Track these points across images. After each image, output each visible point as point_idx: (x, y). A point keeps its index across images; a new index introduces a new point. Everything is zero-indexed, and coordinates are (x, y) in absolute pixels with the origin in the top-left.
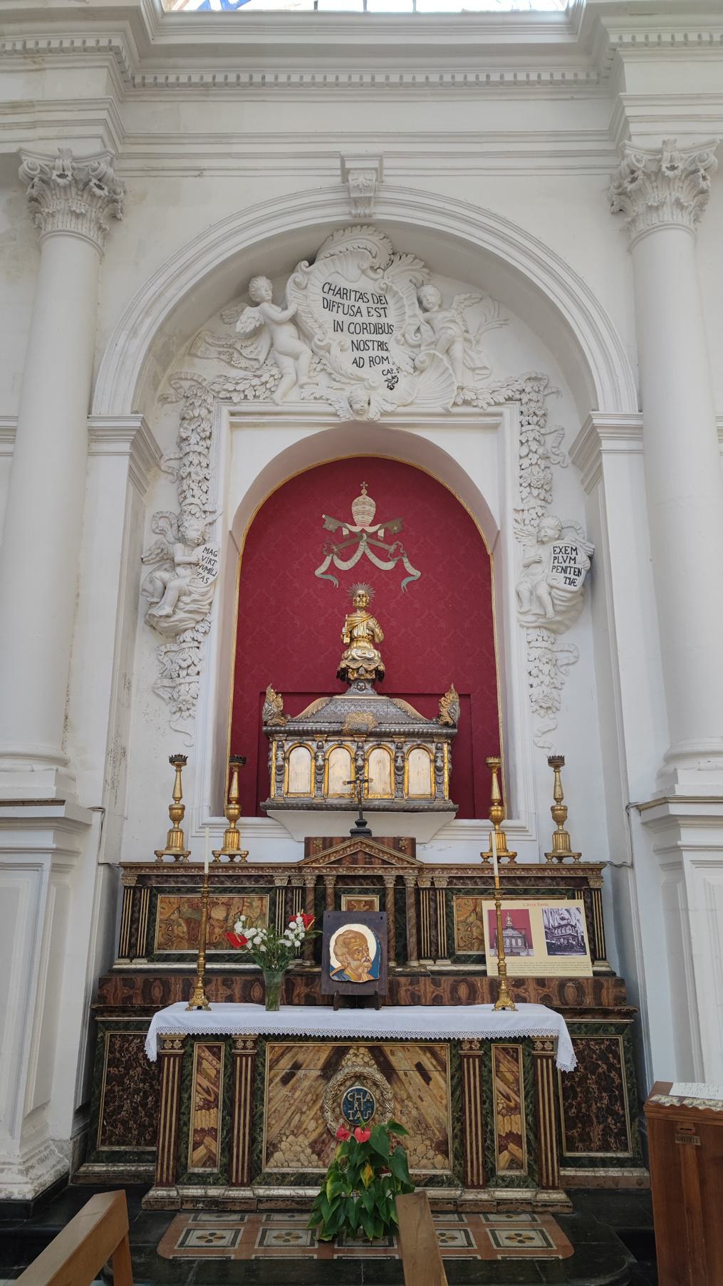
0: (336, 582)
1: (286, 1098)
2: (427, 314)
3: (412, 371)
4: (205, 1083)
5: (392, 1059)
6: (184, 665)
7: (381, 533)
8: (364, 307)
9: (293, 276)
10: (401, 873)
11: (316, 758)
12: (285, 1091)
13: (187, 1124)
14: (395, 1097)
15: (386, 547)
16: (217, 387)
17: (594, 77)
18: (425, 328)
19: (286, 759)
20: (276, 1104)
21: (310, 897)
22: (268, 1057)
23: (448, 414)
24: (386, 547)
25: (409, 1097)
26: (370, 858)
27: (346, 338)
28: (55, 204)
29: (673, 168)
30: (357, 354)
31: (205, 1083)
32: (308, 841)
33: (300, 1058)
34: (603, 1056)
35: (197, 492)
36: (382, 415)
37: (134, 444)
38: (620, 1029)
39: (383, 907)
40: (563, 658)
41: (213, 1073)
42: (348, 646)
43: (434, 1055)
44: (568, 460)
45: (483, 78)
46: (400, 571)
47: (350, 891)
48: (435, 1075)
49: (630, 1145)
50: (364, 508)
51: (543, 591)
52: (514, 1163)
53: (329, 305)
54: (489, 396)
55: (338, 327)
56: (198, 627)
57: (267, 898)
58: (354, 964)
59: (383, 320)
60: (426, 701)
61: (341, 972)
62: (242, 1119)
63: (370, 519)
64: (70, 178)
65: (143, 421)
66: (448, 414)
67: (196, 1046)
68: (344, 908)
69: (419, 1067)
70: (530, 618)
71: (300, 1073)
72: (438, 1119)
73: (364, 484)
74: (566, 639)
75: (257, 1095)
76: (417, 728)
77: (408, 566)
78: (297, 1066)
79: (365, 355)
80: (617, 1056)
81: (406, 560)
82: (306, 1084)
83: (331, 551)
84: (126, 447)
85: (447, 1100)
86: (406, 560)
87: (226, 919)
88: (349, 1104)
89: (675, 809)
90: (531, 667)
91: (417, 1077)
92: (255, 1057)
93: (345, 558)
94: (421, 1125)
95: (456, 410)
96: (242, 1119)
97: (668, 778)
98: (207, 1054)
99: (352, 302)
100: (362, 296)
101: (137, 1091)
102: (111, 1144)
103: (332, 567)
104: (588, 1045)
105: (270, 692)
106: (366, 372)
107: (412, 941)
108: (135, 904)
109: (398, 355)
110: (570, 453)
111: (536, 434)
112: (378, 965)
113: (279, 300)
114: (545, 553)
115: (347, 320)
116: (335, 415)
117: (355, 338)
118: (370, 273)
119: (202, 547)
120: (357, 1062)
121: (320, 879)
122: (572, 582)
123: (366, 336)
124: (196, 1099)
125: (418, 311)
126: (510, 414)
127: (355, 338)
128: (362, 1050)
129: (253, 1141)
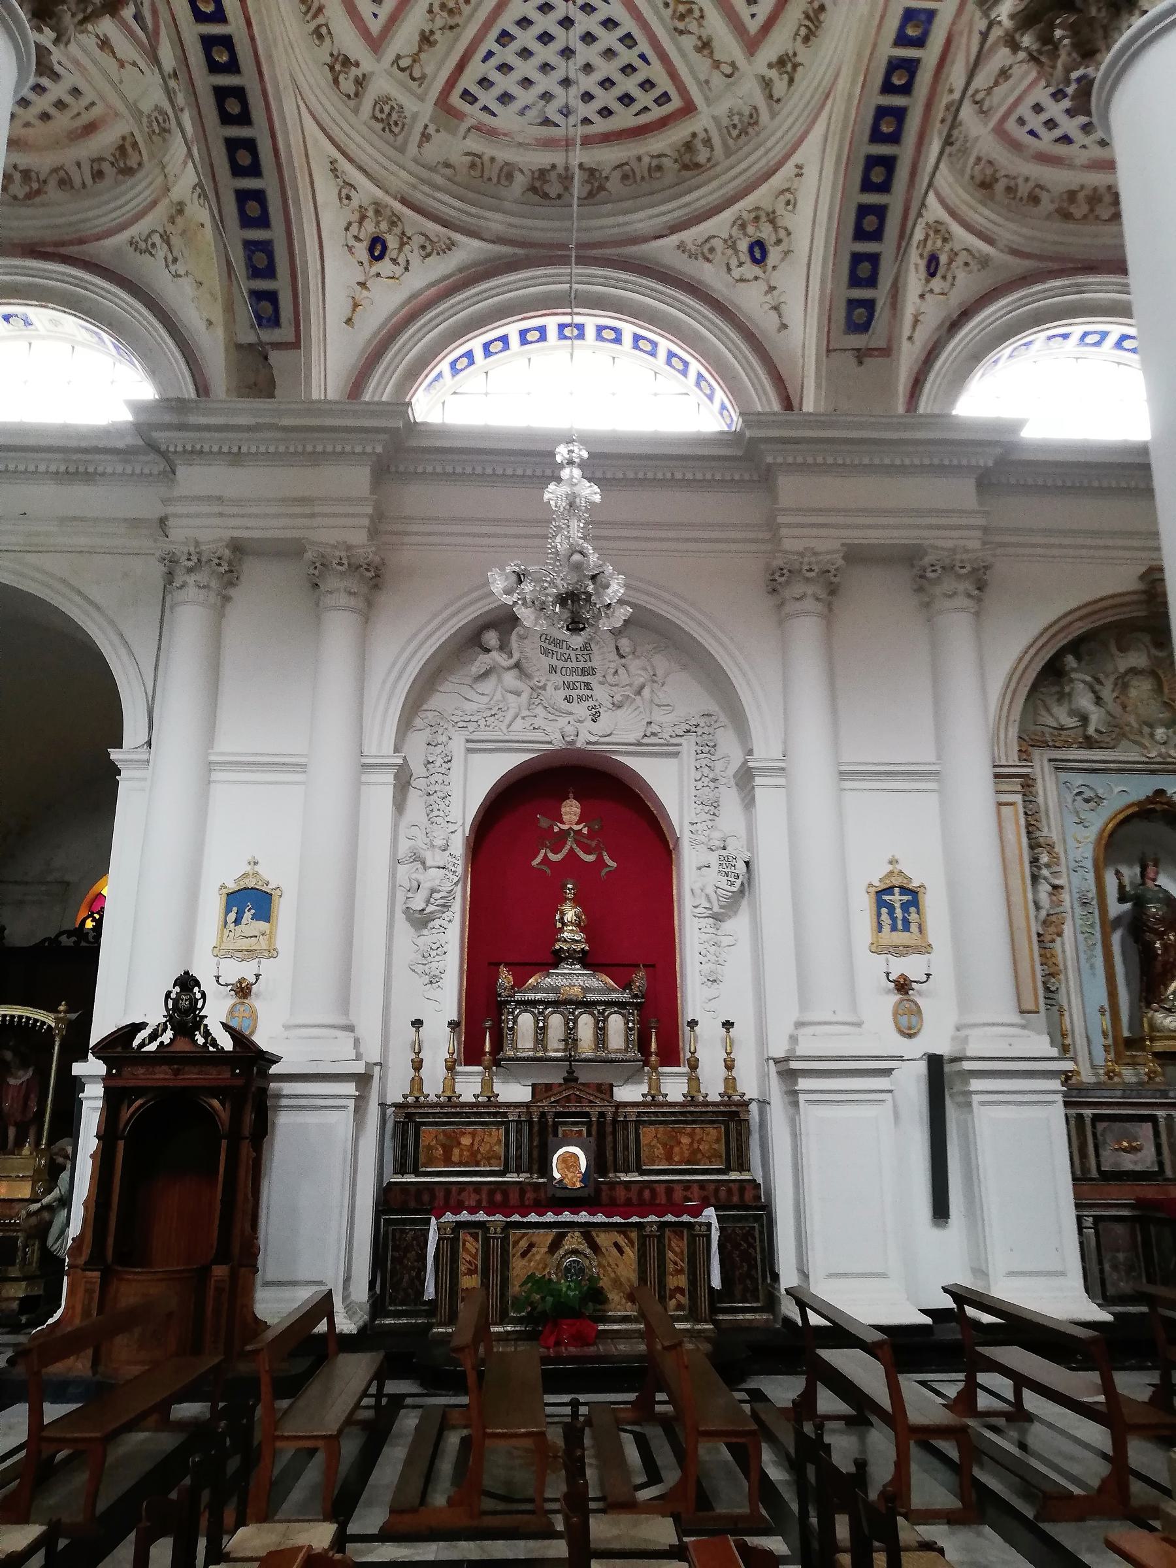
0: (548, 871)
1: (524, 1267)
2: (623, 661)
3: (611, 706)
4: (468, 1258)
5: (597, 1239)
6: (434, 947)
7: (585, 831)
9: (517, 629)
10: (603, 1109)
11: (537, 1021)
12: (524, 1262)
13: (457, 1284)
14: (600, 1265)
15: (589, 842)
16: (455, 718)
17: (756, 478)
18: (622, 671)
19: (515, 1022)
20: (515, 1273)
21: (536, 1128)
22: (512, 1239)
23: (639, 744)
24: (589, 842)
25: (609, 1265)
26: (579, 1099)
27: (558, 679)
28: (331, 582)
29: (811, 570)
30: (568, 692)
31: (468, 1258)
32: (534, 1086)
33: (534, 1239)
35: (442, 806)
36: (588, 743)
37: (396, 776)
39: (589, 1134)
40: (726, 941)
41: (473, 1251)
42: (561, 930)
43: (627, 1237)
44: (733, 782)
45: (669, 476)
46: (600, 862)
47: (565, 1123)
48: (627, 1250)
49: (761, 1297)
50: (571, 811)
51: (710, 890)
52: (679, 1307)
53: (546, 652)
54: (671, 729)
55: (552, 669)
56: (444, 916)
57: (502, 1129)
58: (570, 1175)
59: (589, 664)
60: (620, 972)
61: (561, 1181)
62: (495, 1280)
63: (576, 819)
64: (346, 566)
65: (405, 759)
66: (639, 744)
67: (461, 1232)
68: (560, 1135)
69: (616, 1245)
70: (700, 910)
71: (534, 1250)
72: (629, 1280)
74: (728, 926)
75: (505, 1263)
76: (614, 997)
77: (606, 857)
78: (531, 1246)
79: (574, 693)
80: (754, 1238)
82: (538, 1257)
83: (544, 846)
84: (390, 778)
85: (635, 1266)
87: (472, 1144)
88: (567, 1269)
89: (794, 1065)
90: (701, 948)
91: (615, 1251)
92: (502, 1238)
94: (617, 1283)
95: (646, 740)
96: (495, 1280)
97: (794, 1039)
98: (469, 1238)
99: (564, 650)
101: (413, 1268)
102: (396, 1305)
103: (546, 860)
104: (734, 1230)
105: (503, 970)
107: (610, 1158)
108: (405, 1133)
109: (601, 694)
110: (734, 776)
111: (707, 762)
112: (585, 1177)
113: (504, 647)
114: (713, 858)
115: (560, 664)
116: (550, 743)
117: (567, 679)
119: (447, 853)
120: (573, 1241)
121: (543, 1115)
122: (732, 884)
123: (575, 678)
124: (463, 1268)
125: (617, 657)
126: (688, 745)
127: (567, 679)
128: (577, 1234)
129: (503, 1295)
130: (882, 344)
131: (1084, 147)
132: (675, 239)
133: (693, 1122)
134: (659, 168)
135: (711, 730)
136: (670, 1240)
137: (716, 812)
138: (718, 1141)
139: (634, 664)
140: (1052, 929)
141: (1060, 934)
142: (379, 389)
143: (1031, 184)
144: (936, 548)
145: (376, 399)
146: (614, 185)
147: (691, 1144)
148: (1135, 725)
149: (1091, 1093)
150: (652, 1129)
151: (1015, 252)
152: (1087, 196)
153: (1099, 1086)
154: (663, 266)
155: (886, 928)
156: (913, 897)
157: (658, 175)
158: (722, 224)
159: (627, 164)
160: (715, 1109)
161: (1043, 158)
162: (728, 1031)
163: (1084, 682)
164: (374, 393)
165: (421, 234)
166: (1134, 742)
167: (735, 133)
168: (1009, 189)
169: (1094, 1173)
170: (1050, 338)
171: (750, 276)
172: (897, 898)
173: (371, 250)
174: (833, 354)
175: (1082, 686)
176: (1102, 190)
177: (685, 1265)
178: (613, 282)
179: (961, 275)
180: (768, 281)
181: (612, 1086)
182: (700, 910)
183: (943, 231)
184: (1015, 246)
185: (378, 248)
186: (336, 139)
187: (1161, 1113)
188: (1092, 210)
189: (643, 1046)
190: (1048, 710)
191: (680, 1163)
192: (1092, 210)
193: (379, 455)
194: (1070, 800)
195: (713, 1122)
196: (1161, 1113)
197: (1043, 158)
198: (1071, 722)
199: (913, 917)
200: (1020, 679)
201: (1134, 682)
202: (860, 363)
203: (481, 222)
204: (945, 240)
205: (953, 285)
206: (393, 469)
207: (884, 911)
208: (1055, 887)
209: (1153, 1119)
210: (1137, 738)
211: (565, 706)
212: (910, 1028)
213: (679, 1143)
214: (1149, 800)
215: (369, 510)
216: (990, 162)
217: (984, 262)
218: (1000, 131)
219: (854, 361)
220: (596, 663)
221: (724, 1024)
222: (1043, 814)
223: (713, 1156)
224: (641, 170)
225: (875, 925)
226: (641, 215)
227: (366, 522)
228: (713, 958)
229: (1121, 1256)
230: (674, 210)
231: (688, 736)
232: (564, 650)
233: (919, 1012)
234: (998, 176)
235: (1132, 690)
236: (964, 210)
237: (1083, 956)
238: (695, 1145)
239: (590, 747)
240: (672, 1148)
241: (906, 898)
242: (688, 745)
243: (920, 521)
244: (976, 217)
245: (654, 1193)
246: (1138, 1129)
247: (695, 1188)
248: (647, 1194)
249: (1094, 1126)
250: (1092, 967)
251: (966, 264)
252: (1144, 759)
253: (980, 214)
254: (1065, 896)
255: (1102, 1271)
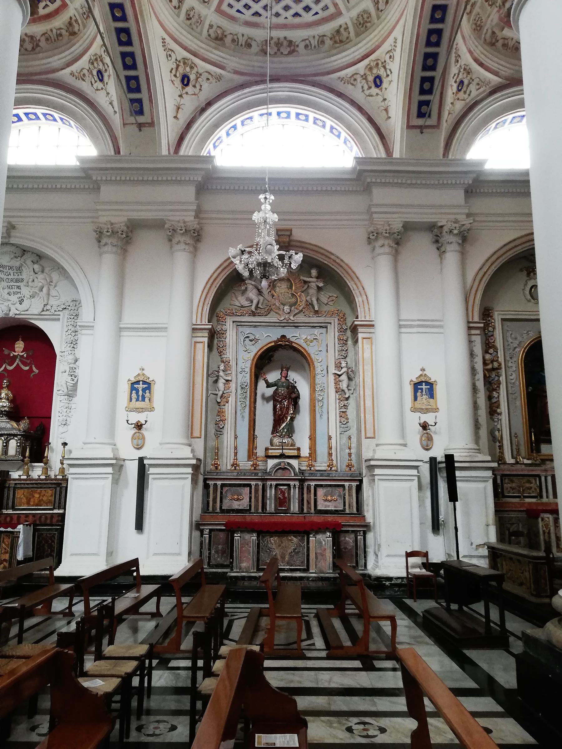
7: (25, 356)
8: (12, 272)
15: (26, 361)
24: (26, 361)
34: (51, 538)
38: (56, 530)
45: (54, 186)
46: (31, 370)
50: (20, 346)
59: (20, 277)
70: (61, 392)
73: (20, 336)
77: (34, 368)
79: (12, 291)
80: (55, 538)
81: (33, 366)
83: (5, 362)
86: (33, 366)
93: (11, 365)
100: (11, 268)
106: (10, 298)
109: (25, 291)
115: (5, 277)
118: (15, 259)
123: (12, 284)
126: (65, 315)
130: (150, 121)
131: (286, 18)
132: (68, 70)
133: (41, 488)
134: (61, 35)
135: (76, 308)
136: (4, 539)
137: (75, 346)
138: (52, 496)
139: (41, 276)
140: (225, 400)
141: (227, 402)
142: (187, 149)
143: (245, 38)
144: (169, 220)
145: (186, 154)
146: (43, 43)
147: (39, 497)
148: (277, 305)
149: (225, 474)
150: (22, 491)
151: (236, 72)
152: (275, 42)
153: (231, 471)
154: (66, 83)
155: (134, 400)
156: (148, 386)
157: (61, 38)
158: (83, 62)
159: (46, 33)
160: (51, 482)
161: (248, 24)
162: (64, 447)
163: (252, 285)
164: (185, 151)
165: (206, 72)
166: (276, 313)
167: (85, 16)
168: (233, 41)
169: (218, 510)
170: (261, 115)
171: (100, 88)
172: (141, 386)
173: (182, 81)
174: (126, 126)
175: (251, 286)
176: (282, 39)
177: (9, 550)
178: (34, 91)
179: (205, 85)
180: (106, 90)
181: (9, 472)
182: (61, 392)
183: (190, 63)
184: (237, 69)
185: (186, 80)
186: (166, 27)
187: (253, 483)
188: (279, 50)
189: (23, 454)
190: (236, 298)
191: (33, 506)
192: (279, 50)
193: (200, 181)
194: (242, 340)
195: (50, 488)
196: (253, 483)
197: (248, 24)
198: (246, 303)
199: (147, 394)
200: (213, 283)
201: (279, 285)
202: (140, 130)
203: (50, 65)
204: (192, 68)
205: (200, 90)
206: (206, 187)
207: (134, 392)
208: (227, 381)
209: (250, 486)
210: (277, 311)
211: (7, 296)
212: (138, 445)
213: (34, 497)
214: (279, 340)
215: (195, 208)
216: (218, 27)
217: (219, 78)
218: (219, 10)
219: (137, 129)
220: (24, 276)
221: (62, 444)
222: (227, 347)
223: (49, 502)
224: (53, 35)
225: (129, 398)
226: (56, 58)
227: (193, 213)
228: (65, 414)
229: (220, 547)
230: (67, 55)
231: (64, 311)
232: (7, 270)
233: (144, 438)
234: (225, 34)
235: (277, 288)
236: (202, 52)
237: (239, 413)
238: (41, 498)
239: (16, 316)
240: (30, 499)
241: (145, 386)
242: (65, 315)
243: (165, 207)
244: (213, 56)
245: (12, 519)
246: (242, 490)
247: (31, 517)
248: (8, 519)
249: (222, 489)
250: (243, 417)
251: (208, 79)
252: (278, 321)
253: (214, 54)
254: (233, 385)
255: (210, 554)
